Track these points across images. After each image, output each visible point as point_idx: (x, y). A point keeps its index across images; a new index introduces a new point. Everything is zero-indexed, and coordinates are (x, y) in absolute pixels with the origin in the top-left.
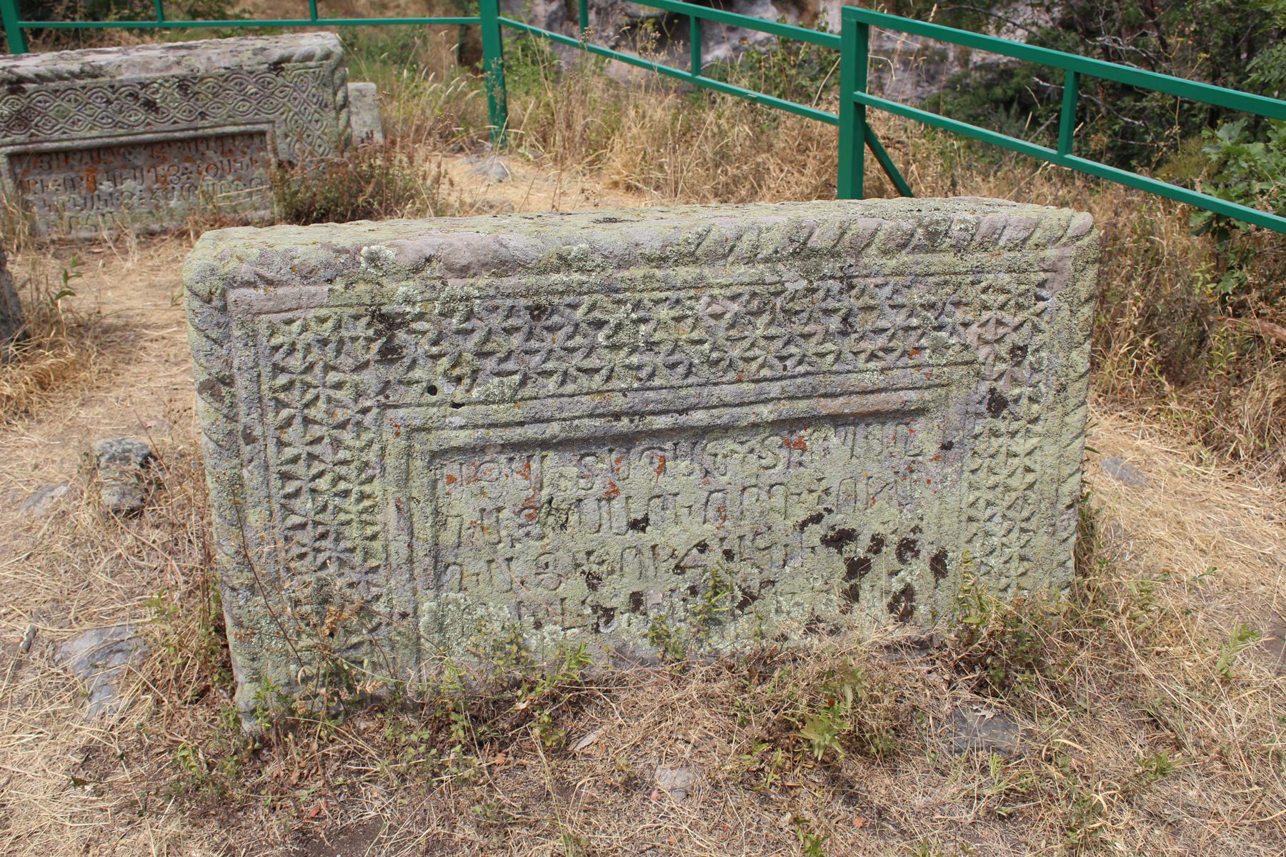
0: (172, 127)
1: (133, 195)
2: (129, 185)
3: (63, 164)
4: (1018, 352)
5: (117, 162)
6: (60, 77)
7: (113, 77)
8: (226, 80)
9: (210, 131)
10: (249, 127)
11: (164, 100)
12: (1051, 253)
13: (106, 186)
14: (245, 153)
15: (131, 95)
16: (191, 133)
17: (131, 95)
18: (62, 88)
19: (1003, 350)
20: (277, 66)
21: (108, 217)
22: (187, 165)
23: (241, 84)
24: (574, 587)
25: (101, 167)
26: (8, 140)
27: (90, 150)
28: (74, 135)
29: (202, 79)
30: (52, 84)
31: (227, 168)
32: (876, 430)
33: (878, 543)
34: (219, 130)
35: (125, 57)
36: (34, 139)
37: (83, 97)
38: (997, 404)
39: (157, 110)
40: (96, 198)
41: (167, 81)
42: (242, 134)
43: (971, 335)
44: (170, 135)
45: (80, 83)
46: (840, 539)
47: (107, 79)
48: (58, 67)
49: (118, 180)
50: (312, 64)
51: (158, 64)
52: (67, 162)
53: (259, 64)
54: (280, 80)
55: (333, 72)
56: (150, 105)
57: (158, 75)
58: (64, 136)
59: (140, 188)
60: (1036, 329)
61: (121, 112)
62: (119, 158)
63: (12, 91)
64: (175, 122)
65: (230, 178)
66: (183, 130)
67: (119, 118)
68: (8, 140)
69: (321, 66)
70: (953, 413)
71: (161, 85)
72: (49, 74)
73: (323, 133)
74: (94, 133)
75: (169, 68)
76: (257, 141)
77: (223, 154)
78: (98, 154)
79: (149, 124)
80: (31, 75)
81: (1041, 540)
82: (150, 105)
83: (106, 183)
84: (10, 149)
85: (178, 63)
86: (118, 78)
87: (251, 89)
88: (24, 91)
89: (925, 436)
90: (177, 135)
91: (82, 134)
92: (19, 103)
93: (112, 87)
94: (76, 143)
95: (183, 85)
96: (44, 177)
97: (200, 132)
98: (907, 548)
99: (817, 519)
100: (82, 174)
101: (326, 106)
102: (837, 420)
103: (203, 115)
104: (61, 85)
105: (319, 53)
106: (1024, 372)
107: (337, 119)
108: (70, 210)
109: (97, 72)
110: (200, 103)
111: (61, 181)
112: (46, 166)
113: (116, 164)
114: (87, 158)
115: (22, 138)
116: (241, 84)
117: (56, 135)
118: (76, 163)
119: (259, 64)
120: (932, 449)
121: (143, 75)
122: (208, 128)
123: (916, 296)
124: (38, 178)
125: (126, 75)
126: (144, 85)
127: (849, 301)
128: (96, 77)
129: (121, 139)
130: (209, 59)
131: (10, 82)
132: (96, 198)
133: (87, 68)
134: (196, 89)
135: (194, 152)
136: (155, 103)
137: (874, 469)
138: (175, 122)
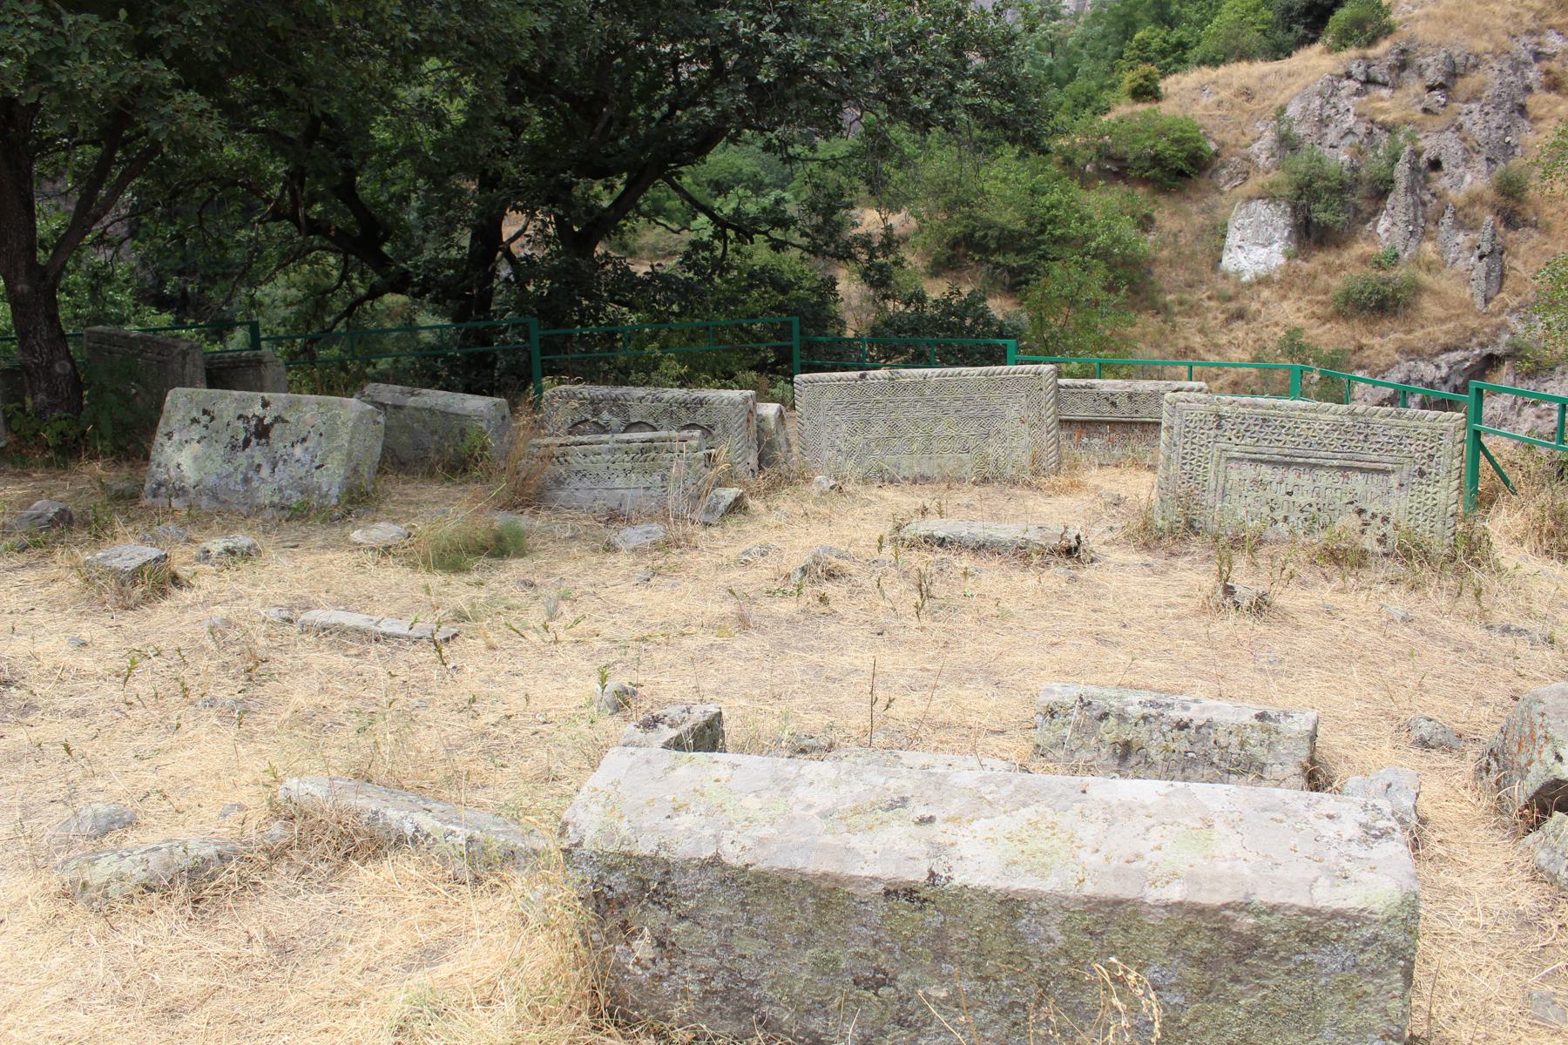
2: (1096, 440)
4: (1431, 457)
5: (1092, 429)
12: (1445, 424)
13: (1085, 440)
19: (1425, 455)
24: (1266, 510)
27: (1081, 422)
32: (1375, 476)
33: (1374, 516)
37: (1084, 397)
38: (1422, 474)
43: (1412, 448)
46: (1361, 512)
56: (1113, 404)
60: (1438, 450)
70: (1405, 474)
78: (1084, 424)
81: (1439, 526)
82: (1113, 404)
89: (1394, 480)
95: (1130, 396)
98: (1385, 520)
99: (1352, 503)
102: (1361, 470)
103: (1137, 411)
104: (1076, 390)
106: (1433, 464)
120: (1396, 485)
122: (1138, 418)
123: (1393, 432)
126: (1112, 395)
127: (1368, 431)
137: (1374, 489)
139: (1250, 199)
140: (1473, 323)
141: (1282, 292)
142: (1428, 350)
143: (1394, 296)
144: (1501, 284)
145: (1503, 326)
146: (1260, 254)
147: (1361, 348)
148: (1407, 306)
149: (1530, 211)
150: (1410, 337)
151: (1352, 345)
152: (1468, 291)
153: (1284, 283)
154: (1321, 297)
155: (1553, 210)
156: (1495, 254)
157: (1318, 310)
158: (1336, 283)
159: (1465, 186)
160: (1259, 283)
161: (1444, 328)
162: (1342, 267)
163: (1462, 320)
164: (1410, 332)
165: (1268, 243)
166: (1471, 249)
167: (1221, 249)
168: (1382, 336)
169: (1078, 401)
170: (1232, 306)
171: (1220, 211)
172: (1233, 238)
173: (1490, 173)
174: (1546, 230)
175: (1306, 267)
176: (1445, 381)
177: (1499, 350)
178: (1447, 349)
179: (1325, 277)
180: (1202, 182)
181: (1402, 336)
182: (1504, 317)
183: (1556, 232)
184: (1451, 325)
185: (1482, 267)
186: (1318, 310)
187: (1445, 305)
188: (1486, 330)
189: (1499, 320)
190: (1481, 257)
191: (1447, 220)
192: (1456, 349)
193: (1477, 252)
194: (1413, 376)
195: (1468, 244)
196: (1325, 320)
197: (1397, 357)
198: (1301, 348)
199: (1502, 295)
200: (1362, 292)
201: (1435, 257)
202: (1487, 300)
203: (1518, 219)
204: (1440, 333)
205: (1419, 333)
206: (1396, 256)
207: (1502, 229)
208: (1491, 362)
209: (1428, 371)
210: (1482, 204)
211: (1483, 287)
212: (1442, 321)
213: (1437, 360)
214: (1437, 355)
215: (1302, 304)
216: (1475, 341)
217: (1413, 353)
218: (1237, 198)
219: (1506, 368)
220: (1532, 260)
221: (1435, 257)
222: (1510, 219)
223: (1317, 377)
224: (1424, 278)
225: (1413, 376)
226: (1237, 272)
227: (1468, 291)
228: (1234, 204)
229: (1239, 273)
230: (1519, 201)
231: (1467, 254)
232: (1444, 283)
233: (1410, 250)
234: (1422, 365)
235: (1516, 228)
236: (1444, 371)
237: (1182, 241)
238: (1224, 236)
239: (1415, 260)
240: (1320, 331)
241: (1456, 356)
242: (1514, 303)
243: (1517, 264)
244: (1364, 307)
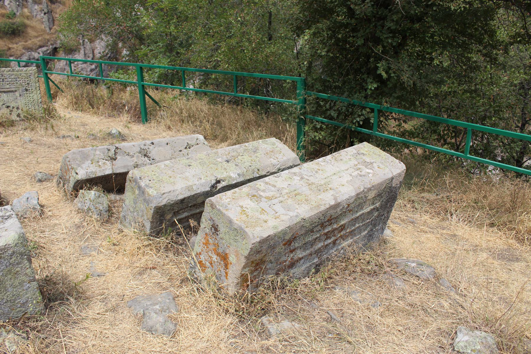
4: (28, 84)
12: (31, 72)
19: (26, 83)
32: (10, 93)
33: (13, 108)
38: (27, 90)
43: (21, 82)
46: (8, 107)
60: (30, 81)
70: (21, 91)
81: (37, 107)
89: (17, 94)
98: (18, 108)
99: (4, 104)
102: (4, 92)
106: (30, 86)
120: (18, 95)
123: (13, 77)
127: (3, 78)
137: (11, 98)
140: (47, 37)
142: (34, 48)
143: (17, 29)
144: (54, 23)
148: (23, 32)
150: (27, 43)
151: (6, 48)
152: (43, 26)
156: (49, 12)
161: (38, 39)
163: (43, 36)
164: (26, 41)
168: (16, 44)
178: (41, 47)
181: (23, 43)
184: (40, 38)
187: (37, 31)
188: (52, 39)
190: (45, 14)
192: (43, 46)
193: (43, 12)
194: (31, 57)
195: (39, 9)
197: (24, 51)
199: (55, 27)
200: (5, 28)
201: (29, 14)
202: (50, 29)
204: (37, 41)
205: (30, 42)
206: (15, 14)
207: (50, 4)
212: (36, 37)
214: (38, 49)
216: (49, 43)
217: (29, 49)
224: (27, 22)
225: (31, 57)
227: (43, 26)
231: (40, 13)
234: (33, 53)
235: (54, 3)
239: (22, 15)
241: (44, 49)
243: (57, 16)
244: (7, 33)
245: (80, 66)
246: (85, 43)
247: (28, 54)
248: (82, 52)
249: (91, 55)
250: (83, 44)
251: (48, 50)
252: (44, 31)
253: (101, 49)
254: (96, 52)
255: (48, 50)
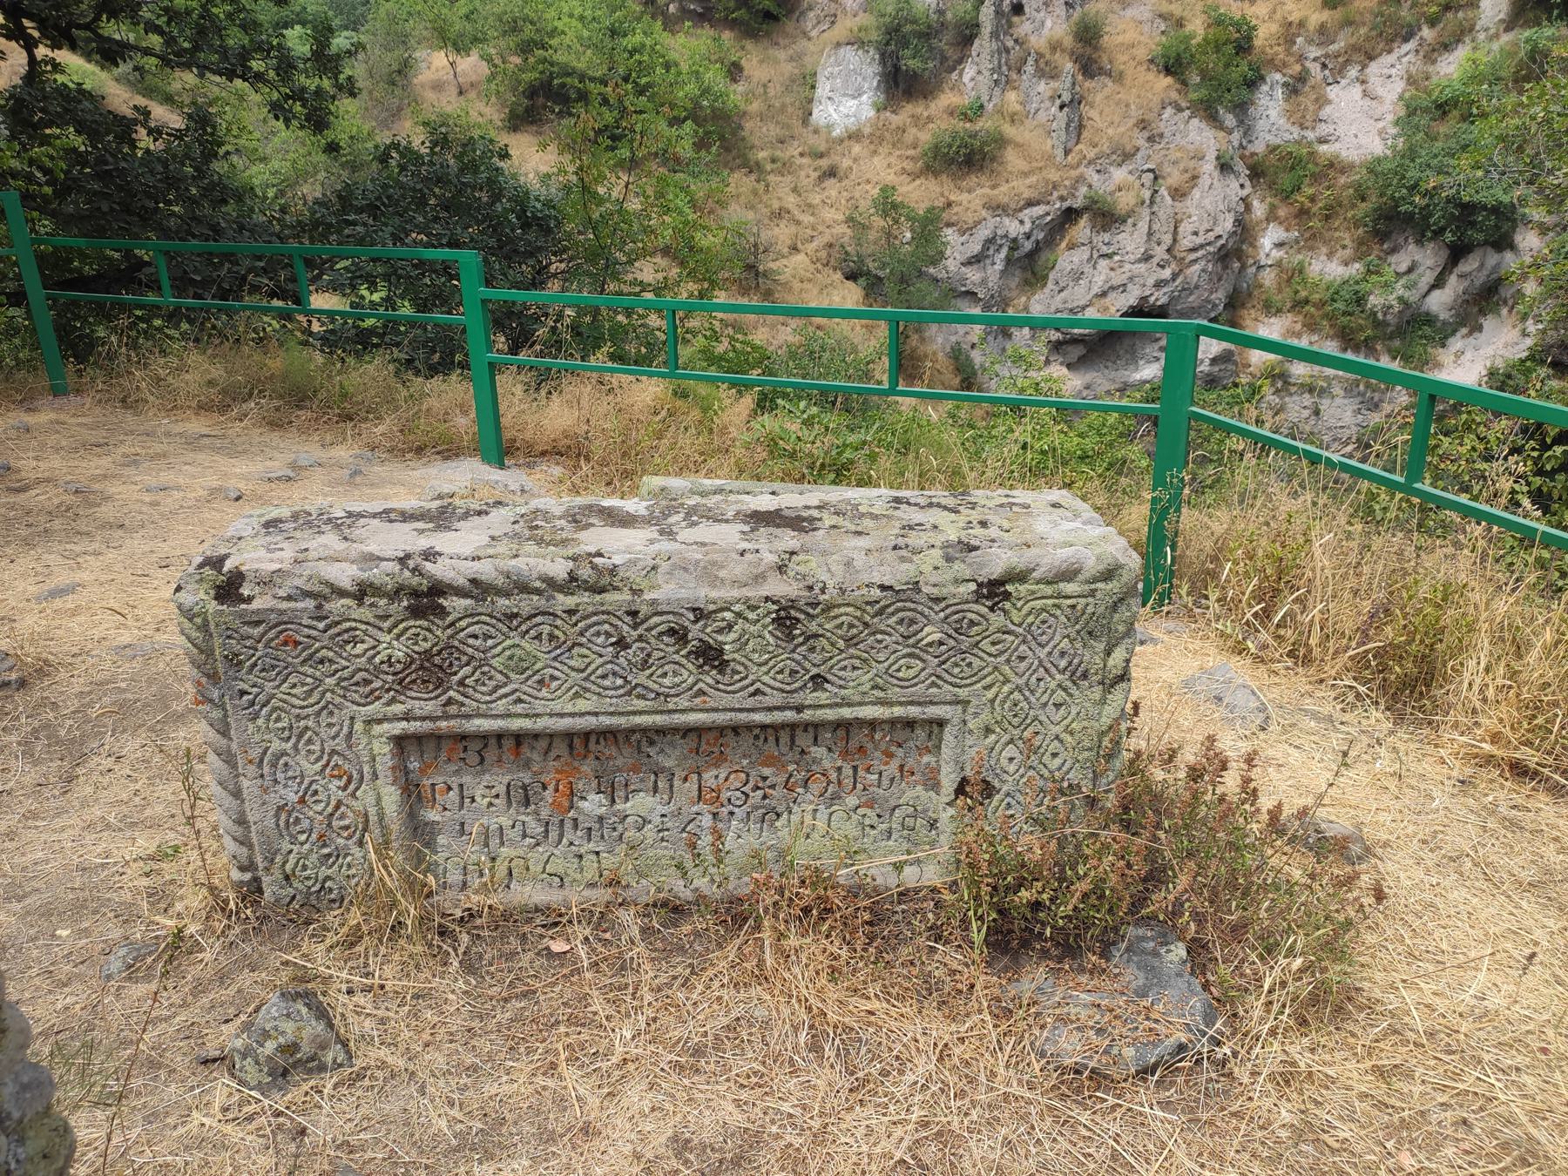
0: (749, 703)
1: (645, 821)
2: (642, 803)
3: (508, 756)
5: (622, 758)
6: (524, 588)
7: (637, 592)
8: (880, 612)
9: (830, 715)
10: (914, 711)
11: (741, 643)
13: (593, 804)
14: (891, 755)
15: (672, 632)
16: (790, 715)
17: (672, 632)
18: (525, 612)
20: (994, 591)
21: (590, 862)
22: (767, 771)
23: (912, 622)
25: (587, 767)
26: (398, 708)
28: (539, 707)
29: (829, 607)
30: (502, 602)
31: (848, 782)
34: (847, 713)
35: (665, 546)
36: (453, 709)
39: (722, 666)
40: (568, 825)
41: (753, 608)
42: (893, 722)
44: (743, 717)
45: (564, 601)
47: (626, 596)
48: (519, 564)
49: (620, 793)
50: (1070, 588)
51: (739, 569)
52: (518, 754)
53: (958, 582)
54: (997, 619)
55: (1115, 607)
56: (710, 656)
57: (735, 593)
58: (519, 708)
59: (665, 810)
61: (645, 664)
62: (627, 751)
63: (416, 612)
64: (757, 692)
65: (852, 801)
66: (770, 709)
67: (642, 678)
68: (398, 708)
69: (1092, 593)
71: (739, 615)
72: (500, 581)
73: (1067, 730)
74: (582, 705)
75: (759, 578)
76: (921, 733)
77: (845, 754)
78: (580, 742)
79: (702, 693)
80: (461, 582)
82: (710, 656)
83: (592, 797)
84: (399, 728)
85: (781, 569)
86: (648, 596)
87: (932, 634)
88: (442, 612)
90: (758, 717)
91: (557, 706)
92: (430, 635)
93: (634, 614)
94: (541, 724)
95: (786, 618)
96: (467, 779)
97: (807, 715)
100: (544, 778)
101: (1085, 676)
103: (818, 681)
104: (525, 604)
105: (1091, 566)
107: (1103, 701)
108: (513, 843)
109: (605, 580)
110: (816, 657)
111: (502, 789)
112: (473, 758)
113: (619, 762)
114: (560, 748)
115: (430, 707)
116: (912, 622)
117: (501, 706)
118: (536, 756)
119: (958, 582)
121: (704, 594)
122: (823, 706)
124: (454, 782)
125: (669, 591)
126: (700, 614)
128: (602, 591)
129: (638, 720)
130: (848, 564)
131: (415, 593)
132: (568, 825)
133: (585, 573)
134: (813, 627)
135: (784, 749)
136: (721, 652)
138: (757, 692)
139: (838, 45)
140: (1054, 176)
141: (872, 147)
143: (981, 150)
144: (1079, 135)
145: (1080, 179)
146: (850, 105)
147: (949, 205)
148: (993, 159)
149: (1105, 59)
150: (996, 192)
151: (940, 203)
152: (1049, 142)
153: (874, 137)
154: (911, 152)
155: (1125, 58)
156: (1073, 103)
157: (908, 166)
158: (925, 137)
159: (1046, 32)
160: (850, 137)
161: (1028, 181)
162: (930, 119)
163: (1044, 172)
164: (994, 187)
165: (857, 94)
166: (1052, 98)
167: (811, 101)
169: (540, 652)
170: (824, 163)
171: (807, 60)
172: (823, 89)
173: (1068, 17)
174: (1119, 78)
175: (896, 120)
176: (1028, 236)
177: (1078, 203)
178: (1030, 204)
179: (914, 130)
180: (790, 26)
181: (987, 191)
182: (1082, 169)
183: (1128, 81)
184: (1033, 179)
185: (1062, 116)
186: (908, 166)
187: (1029, 158)
188: (1067, 183)
189: (1074, 173)
190: (1062, 107)
191: (1029, 68)
192: (1038, 203)
193: (1058, 102)
194: (999, 232)
195: (1049, 93)
196: (915, 176)
197: (984, 213)
198: (895, 206)
199: (1079, 146)
200: (950, 146)
201: (1018, 107)
202: (1067, 152)
203: (1095, 67)
204: (1023, 188)
205: (1004, 188)
206: (982, 106)
208: (1070, 215)
209: (1013, 228)
210: (1063, 51)
211: (1063, 138)
212: (1026, 174)
213: (1021, 215)
214: (1021, 210)
215: (892, 160)
216: (1056, 194)
217: (999, 209)
218: (825, 44)
219: (1084, 221)
220: (1107, 110)
221: (1018, 107)
222: (1089, 67)
223: (908, 235)
224: (1009, 130)
225: (999, 232)
226: (828, 126)
227: (1049, 142)
228: (822, 52)
229: (830, 127)
230: (1096, 48)
231: (1048, 104)
232: (1027, 135)
233: (995, 100)
234: (1006, 221)
235: (1092, 77)
236: (1027, 227)
237: (771, 92)
238: (813, 87)
239: (1000, 111)
240: (910, 188)
241: (1039, 210)
242: (1091, 154)
243: (1093, 113)
244: (952, 161)
245: (1127, 266)
246: (1158, 199)
247: (992, 222)
248: (1143, 226)
249: (1168, 239)
250: (1152, 202)
251: (1048, 214)
252: (1051, 158)
253: (1201, 220)
254: (1185, 228)
255: (1048, 214)
